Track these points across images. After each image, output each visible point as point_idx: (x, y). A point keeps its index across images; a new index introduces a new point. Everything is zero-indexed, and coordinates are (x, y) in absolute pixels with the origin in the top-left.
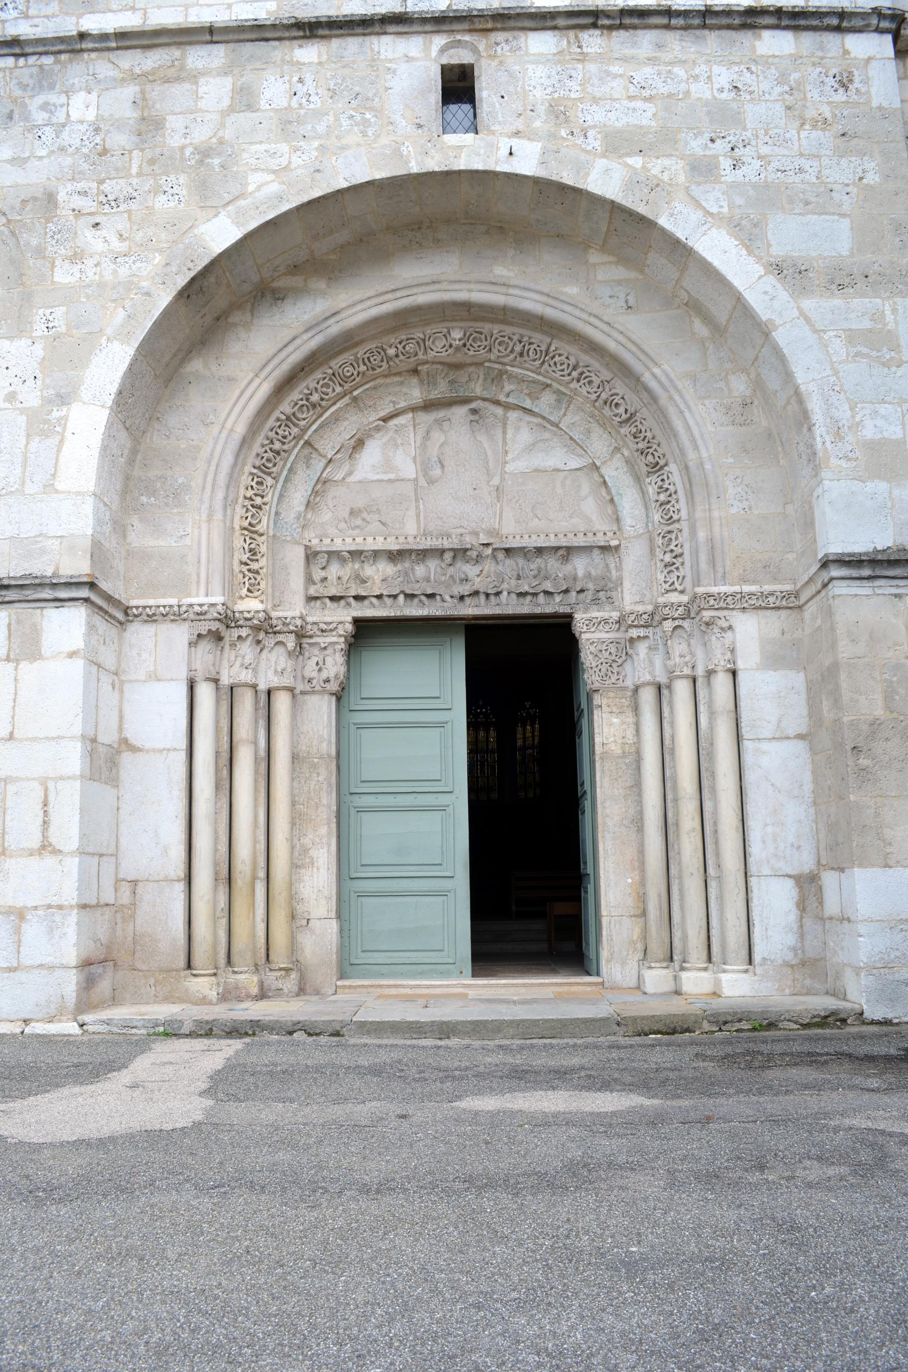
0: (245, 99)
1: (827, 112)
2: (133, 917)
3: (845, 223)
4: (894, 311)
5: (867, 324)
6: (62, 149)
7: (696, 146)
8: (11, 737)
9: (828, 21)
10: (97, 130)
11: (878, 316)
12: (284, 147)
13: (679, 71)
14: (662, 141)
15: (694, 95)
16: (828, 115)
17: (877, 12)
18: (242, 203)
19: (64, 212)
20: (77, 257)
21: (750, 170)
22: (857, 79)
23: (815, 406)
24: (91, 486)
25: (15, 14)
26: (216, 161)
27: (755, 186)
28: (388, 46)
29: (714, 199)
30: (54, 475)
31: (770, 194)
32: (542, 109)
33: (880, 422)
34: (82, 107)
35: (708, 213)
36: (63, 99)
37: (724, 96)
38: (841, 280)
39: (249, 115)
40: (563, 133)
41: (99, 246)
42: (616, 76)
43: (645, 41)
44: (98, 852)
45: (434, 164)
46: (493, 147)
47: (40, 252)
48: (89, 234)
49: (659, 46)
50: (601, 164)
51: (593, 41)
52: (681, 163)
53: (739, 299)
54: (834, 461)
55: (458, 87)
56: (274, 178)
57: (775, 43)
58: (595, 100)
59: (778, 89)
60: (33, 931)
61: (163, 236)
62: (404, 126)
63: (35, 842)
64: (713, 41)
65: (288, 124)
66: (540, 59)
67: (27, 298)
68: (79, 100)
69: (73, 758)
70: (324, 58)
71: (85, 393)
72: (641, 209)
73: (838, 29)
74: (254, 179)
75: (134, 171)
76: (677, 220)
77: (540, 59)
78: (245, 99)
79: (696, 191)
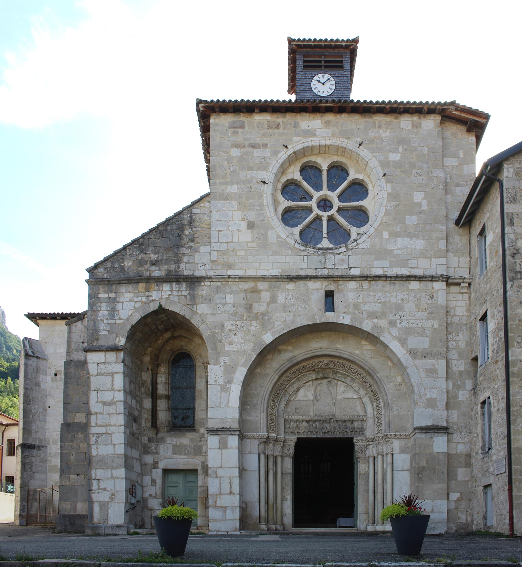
0: (273, 300)
1: (426, 306)
2: (246, 511)
3: (428, 339)
4: (438, 364)
5: (430, 367)
6: (225, 312)
7: (391, 316)
8: (221, 467)
9: (428, 279)
10: (234, 306)
11: (434, 365)
12: (284, 315)
13: (388, 294)
14: (383, 315)
15: (392, 301)
16: (426, 307)
17: (442, 276)
18: (274, 330)
19: (226, 330)
20: (230, 343)
21: (404, 324)
22: (435, 296)
23: (416, 389)
24: (238, 405)
25: (208, 268)
26: (267, 318)
27: (405, 328)
28: (312, 285)
29: (395, 332)
30: (228, 402)
31: (409, 331)
32: (352, 305)
33: (431, 393)
34: (230, 299)
35: (394, 336)
36: (224, 296)
37: (400, 302)
38: (425, 355)
39: (275, 304)
40: (357, 313)
41: (236, 340)
42: (371, 296)
43: (380, 283)
44: (241, 494)
45: (323, 321)
46: (338, 316)
47: (221, 341)
48: (233, 336)
49: (383, 286)
50: (366, 321)
51: (366, 284)
52: (387, 321)
53: (399, 359)
54: (419, 403)
55: (330, 295)
56: (282, 323)
57: (414, 285)
58: (366, 303)
59: (414, 299)
60: (228, 512)
61: (253, 338)
62: (316, 310)
63: (228, 491)
64: (398, 284)
65: (285, 308)
66: (352, 290)
67: (218, 353)
68: (228, 296)
69: (236, 472)
70: (294, 288)
71: (235, 381)
72: (376, 335)
73: (431, 281)
74: (277, 324)
75: (245, 319)
76: (385, 338)
77: (352, 290)
78: (273, 300)
79: (390, 330)
